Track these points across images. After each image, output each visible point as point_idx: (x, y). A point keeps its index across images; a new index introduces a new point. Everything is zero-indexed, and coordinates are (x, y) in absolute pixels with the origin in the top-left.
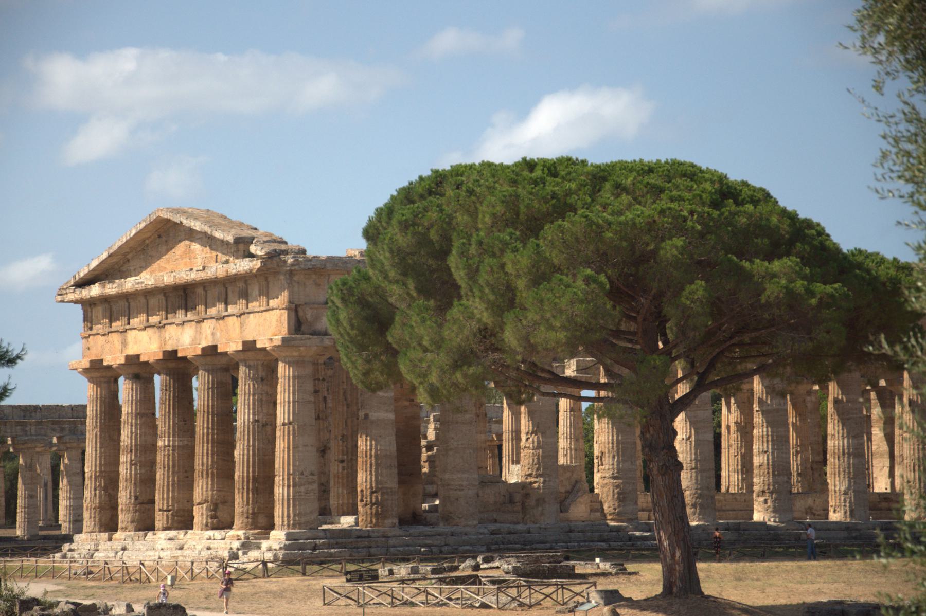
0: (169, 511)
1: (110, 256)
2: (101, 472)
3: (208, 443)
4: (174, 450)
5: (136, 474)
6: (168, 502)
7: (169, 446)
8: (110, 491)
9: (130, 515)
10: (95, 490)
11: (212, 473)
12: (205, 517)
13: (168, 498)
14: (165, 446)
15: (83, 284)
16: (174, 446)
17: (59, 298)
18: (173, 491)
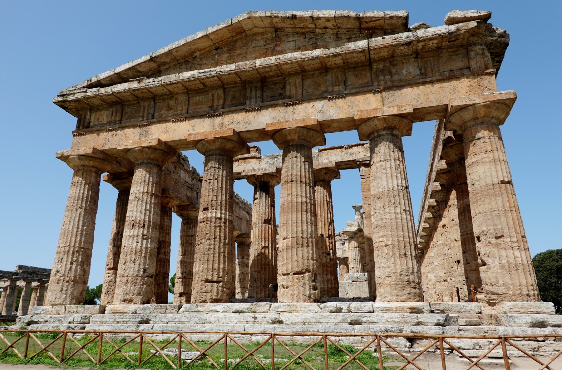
0: (218, 282)
1: (152, 60)
2: (80, 248)
3: (306, 211)
4: (225, 223)
5: (146, 248)
6: (218, 274)
7: (220, 218)
8: (85, 267)
9: (137, 288)
10: (71, 264)
11: (312, 242)
12: (307, 287)
13: (219, 269)
14: (217, 218)
15: (99, 84)
16: (225, 219)
17: (60, 99)
18: (224, 263)
